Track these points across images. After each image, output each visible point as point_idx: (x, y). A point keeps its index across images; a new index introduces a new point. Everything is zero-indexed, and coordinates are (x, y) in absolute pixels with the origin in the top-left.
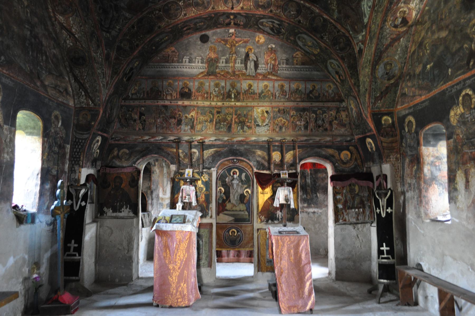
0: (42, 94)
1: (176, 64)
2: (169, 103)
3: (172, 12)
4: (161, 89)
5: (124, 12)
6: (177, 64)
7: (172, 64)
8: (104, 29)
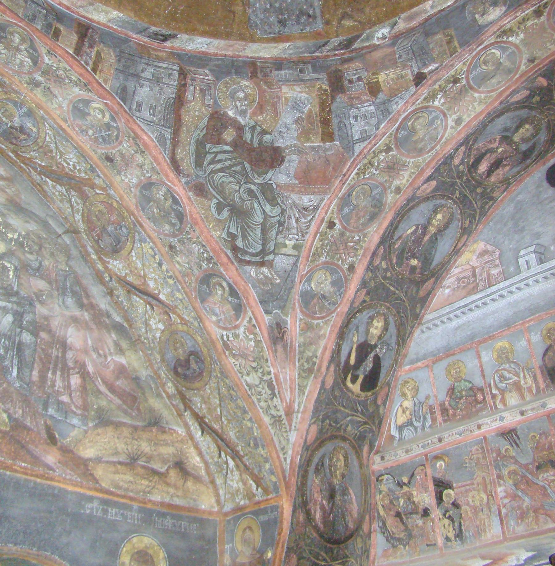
0: (70, 488)
1: (501, 286)
2: (519, 418)
3: (421, 133)
4: (478, 381)
5: (295, 197)
6: (507, 283)
7: (489, 291)
8: (247, 258)
